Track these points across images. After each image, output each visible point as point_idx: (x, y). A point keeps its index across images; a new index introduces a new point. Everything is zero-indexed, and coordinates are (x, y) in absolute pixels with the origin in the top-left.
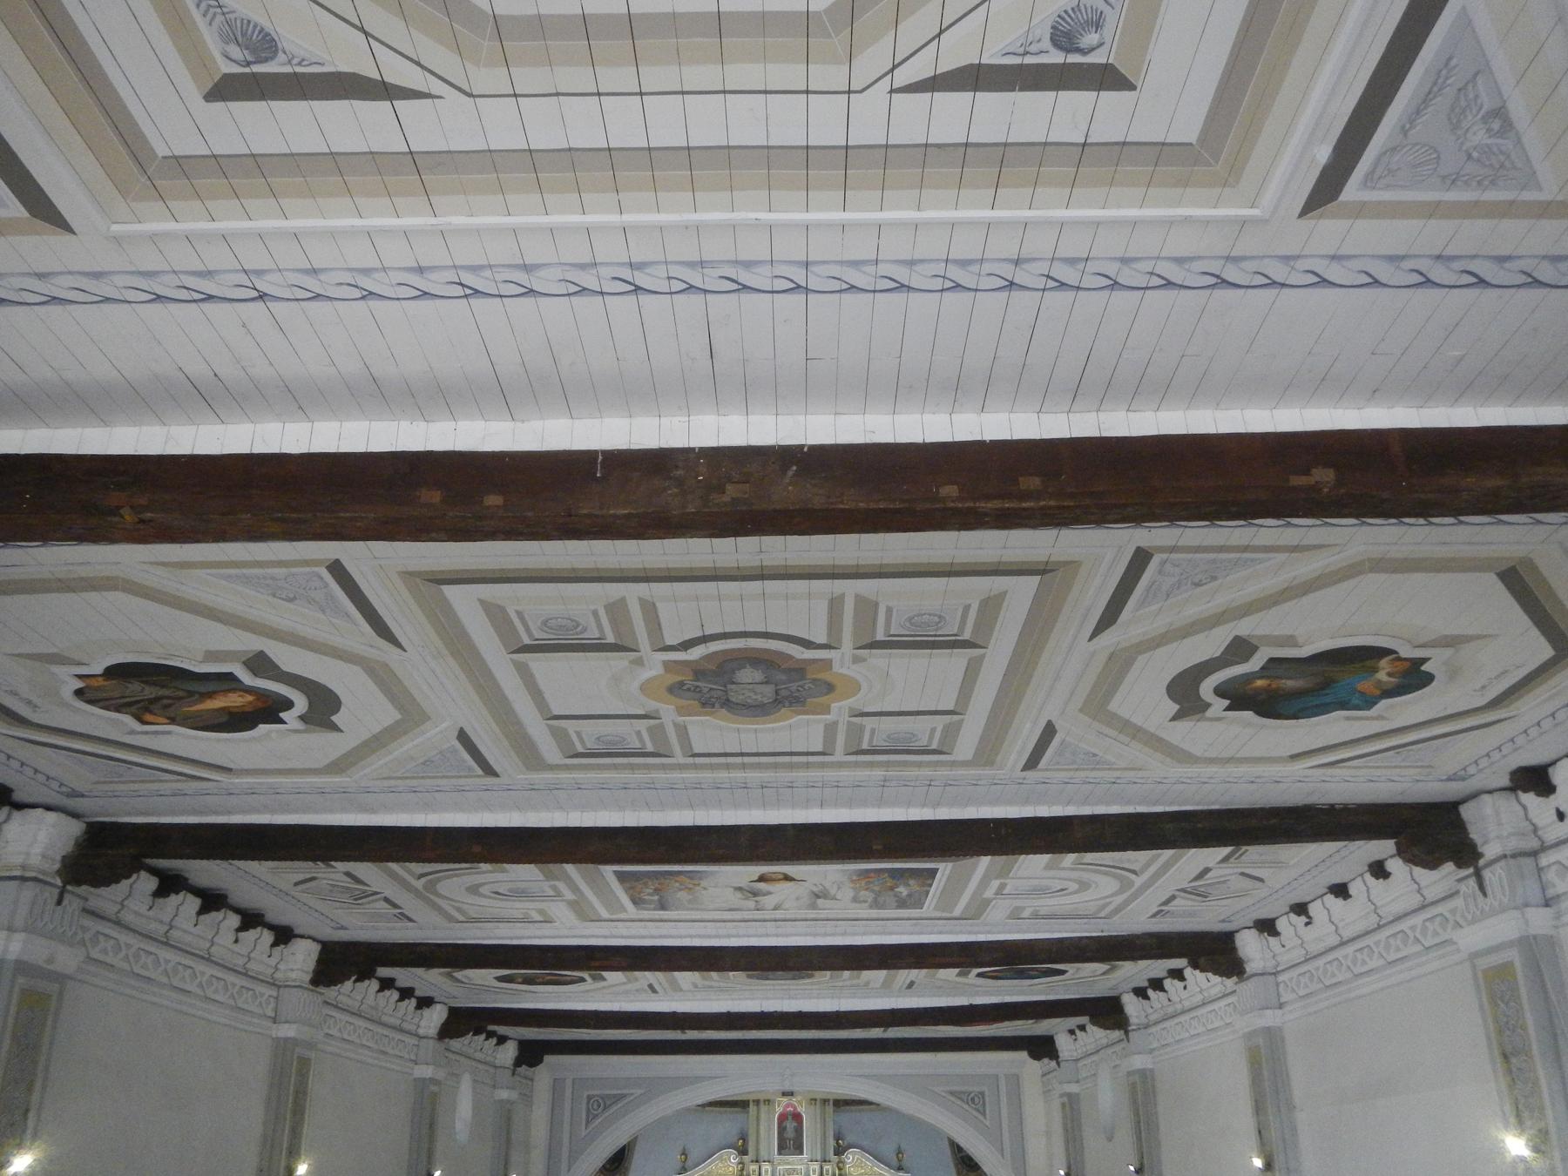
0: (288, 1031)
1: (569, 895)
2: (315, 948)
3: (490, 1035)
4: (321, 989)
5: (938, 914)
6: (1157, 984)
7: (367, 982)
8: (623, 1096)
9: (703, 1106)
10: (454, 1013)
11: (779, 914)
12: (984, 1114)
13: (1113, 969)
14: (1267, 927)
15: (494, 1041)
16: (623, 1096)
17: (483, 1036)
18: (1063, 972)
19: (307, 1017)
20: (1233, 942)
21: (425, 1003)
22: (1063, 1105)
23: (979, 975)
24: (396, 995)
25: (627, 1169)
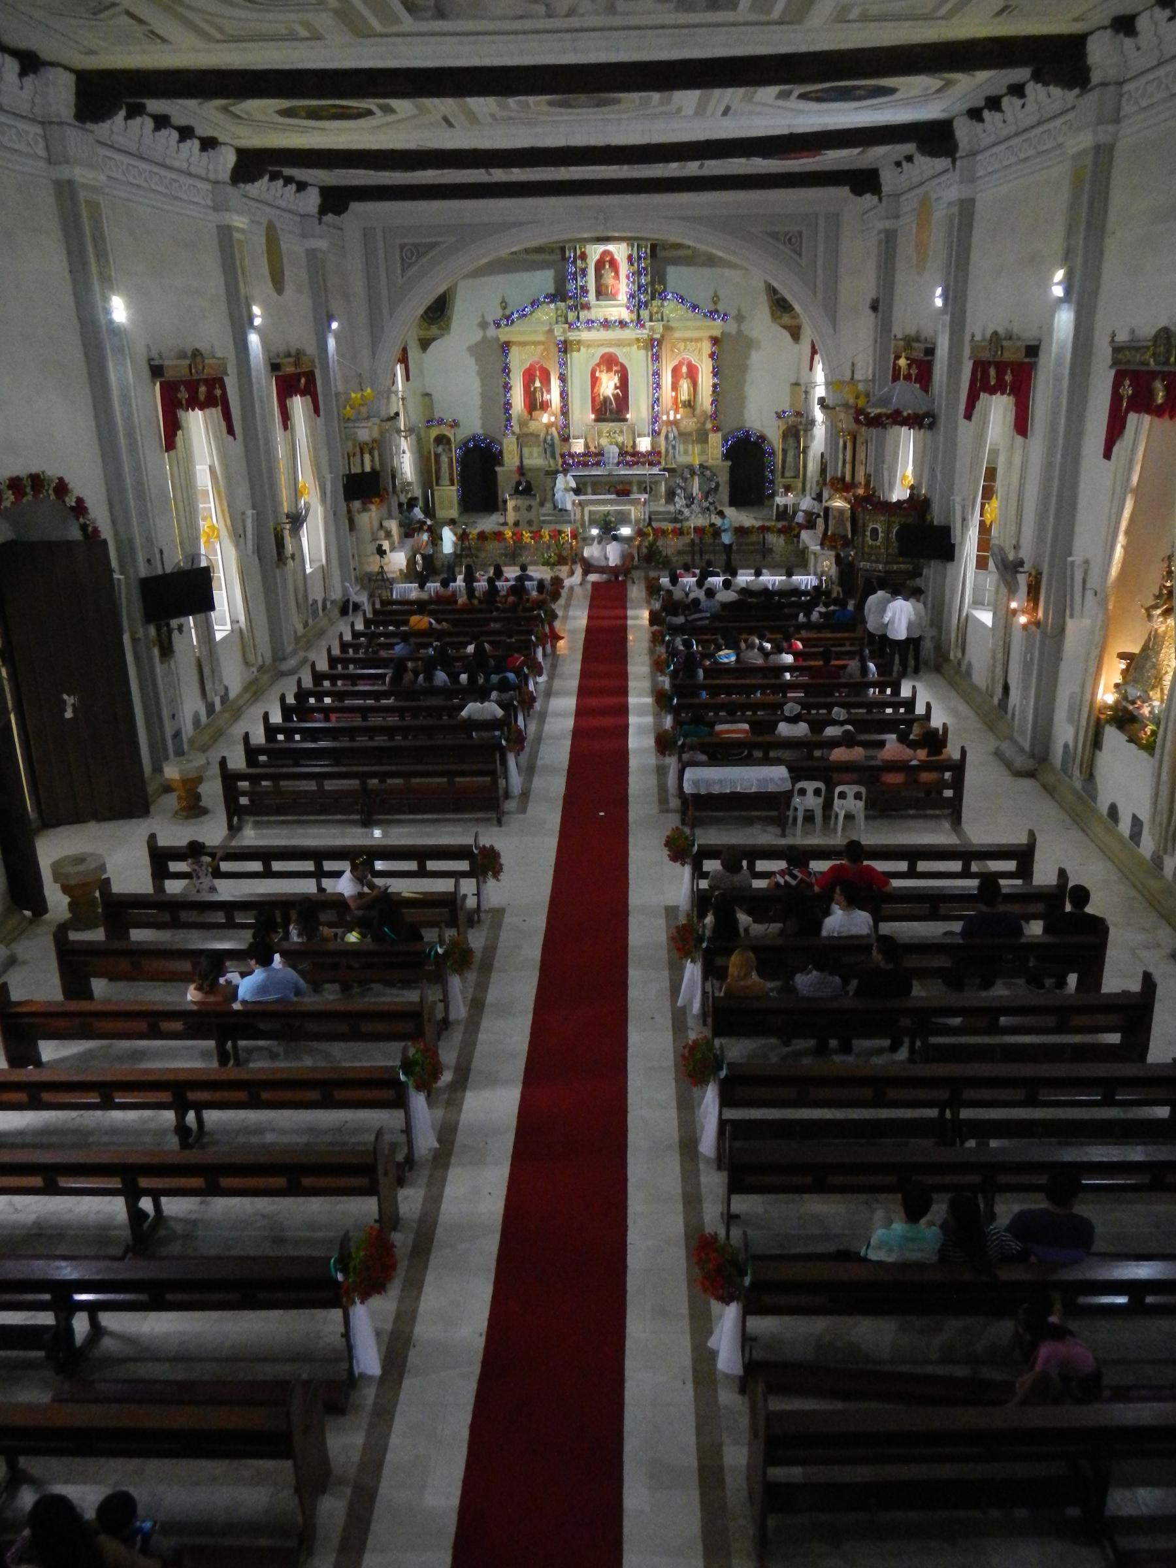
2: (69, 79)
3: (288, 180)
4: (89, 126)
5: (753, 17)
6: (994, 103)
7: (139, 120)
8: (433, 246)
10: (241, 153)
11: (574, 22)
12: (800, 255)
13: (948, 84)
14: (1125, 25)
15: (294, 187)
16: (433, 246)
17: (281, 182)
21: (209, 144)
22: (880, 242)
24: (175, 135)
25: (450, 318)
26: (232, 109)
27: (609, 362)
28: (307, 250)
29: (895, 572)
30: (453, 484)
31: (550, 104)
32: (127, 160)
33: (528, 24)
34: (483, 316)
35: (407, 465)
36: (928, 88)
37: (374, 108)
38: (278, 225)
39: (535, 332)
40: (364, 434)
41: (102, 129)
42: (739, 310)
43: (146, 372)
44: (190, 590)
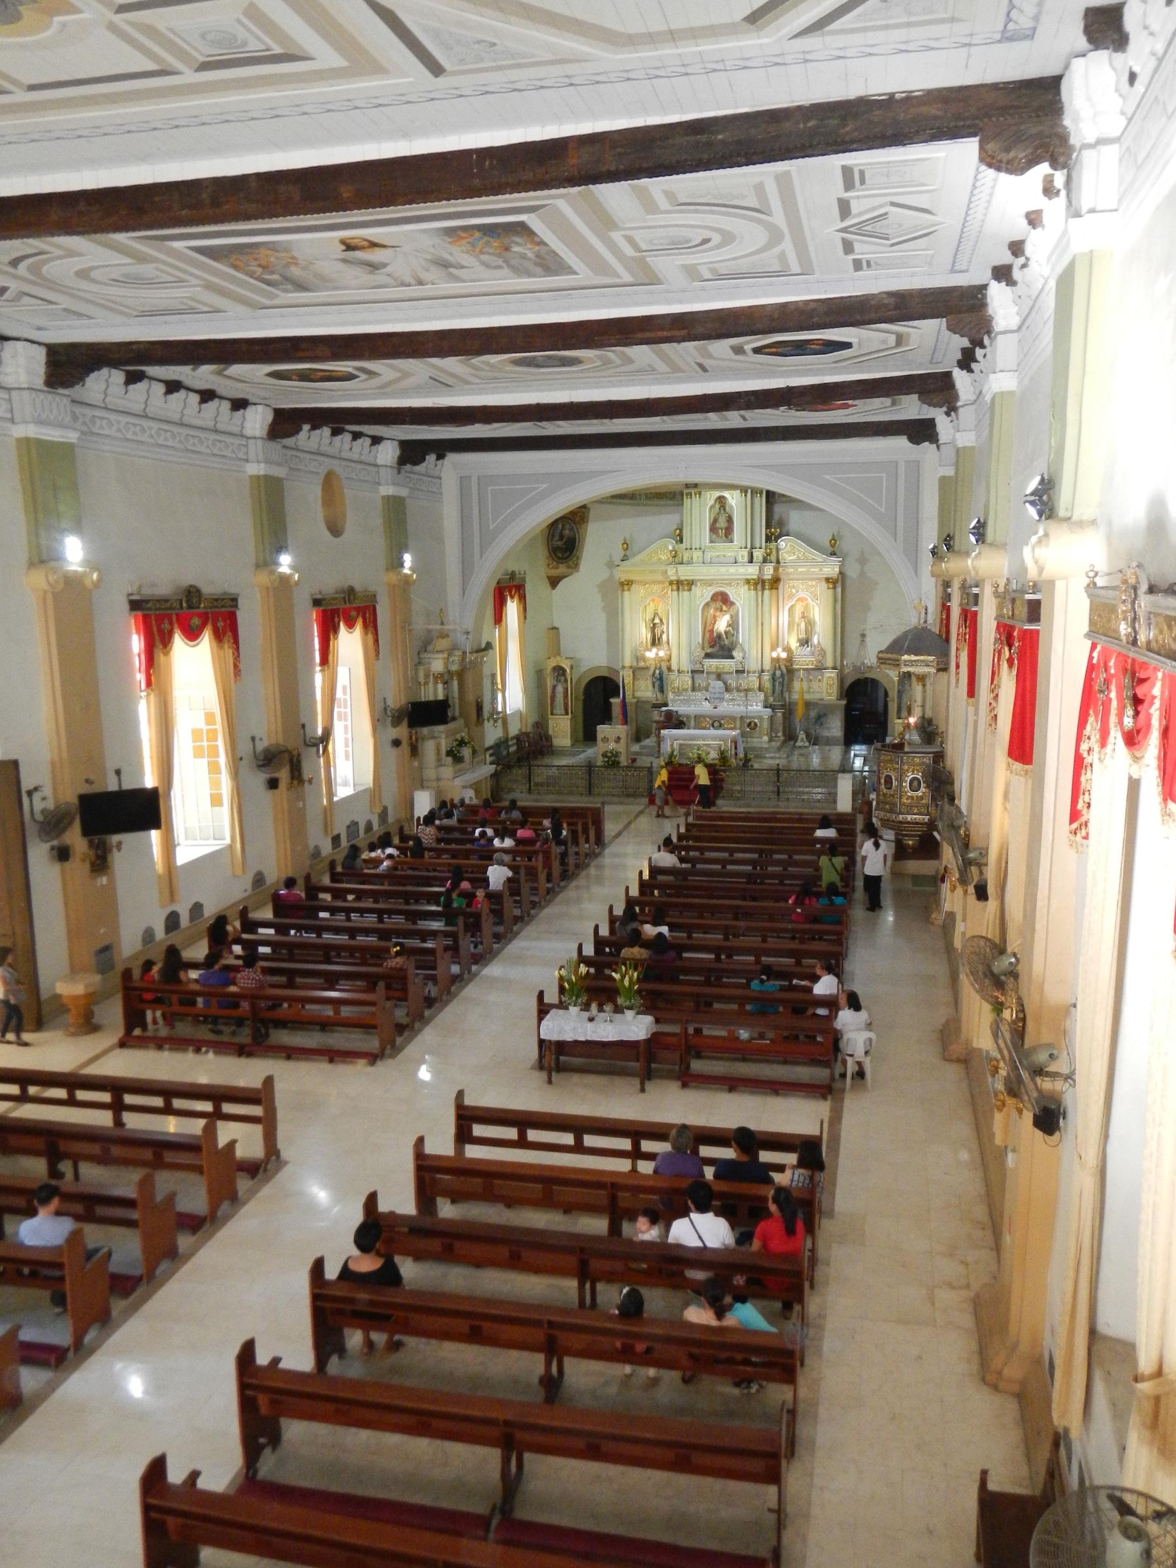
0: (31, 431)
1: (194, 281)
2: (41, 354)
3: (356, 436)
9: (613, 497)
10: (279, 414)
14: (1003, 273)
15: (368, 441)
17: (347, 437)
18: (848, 345)
19: (44, 419)
20: (985, 296)
21: (239, 404)
23: (757, 351)
24: (195, 398)
25: (578, 558)
27: (722, 599)
29: (908, 823)
30: (567, 714)
31: (517, 363)
32: (124, 419)
34: (611, 557)
35: (513, 697)
36: (884, 342)
41: (76, 391)
42: (862, 553)
43: (127, 607)
44: (145, 810)
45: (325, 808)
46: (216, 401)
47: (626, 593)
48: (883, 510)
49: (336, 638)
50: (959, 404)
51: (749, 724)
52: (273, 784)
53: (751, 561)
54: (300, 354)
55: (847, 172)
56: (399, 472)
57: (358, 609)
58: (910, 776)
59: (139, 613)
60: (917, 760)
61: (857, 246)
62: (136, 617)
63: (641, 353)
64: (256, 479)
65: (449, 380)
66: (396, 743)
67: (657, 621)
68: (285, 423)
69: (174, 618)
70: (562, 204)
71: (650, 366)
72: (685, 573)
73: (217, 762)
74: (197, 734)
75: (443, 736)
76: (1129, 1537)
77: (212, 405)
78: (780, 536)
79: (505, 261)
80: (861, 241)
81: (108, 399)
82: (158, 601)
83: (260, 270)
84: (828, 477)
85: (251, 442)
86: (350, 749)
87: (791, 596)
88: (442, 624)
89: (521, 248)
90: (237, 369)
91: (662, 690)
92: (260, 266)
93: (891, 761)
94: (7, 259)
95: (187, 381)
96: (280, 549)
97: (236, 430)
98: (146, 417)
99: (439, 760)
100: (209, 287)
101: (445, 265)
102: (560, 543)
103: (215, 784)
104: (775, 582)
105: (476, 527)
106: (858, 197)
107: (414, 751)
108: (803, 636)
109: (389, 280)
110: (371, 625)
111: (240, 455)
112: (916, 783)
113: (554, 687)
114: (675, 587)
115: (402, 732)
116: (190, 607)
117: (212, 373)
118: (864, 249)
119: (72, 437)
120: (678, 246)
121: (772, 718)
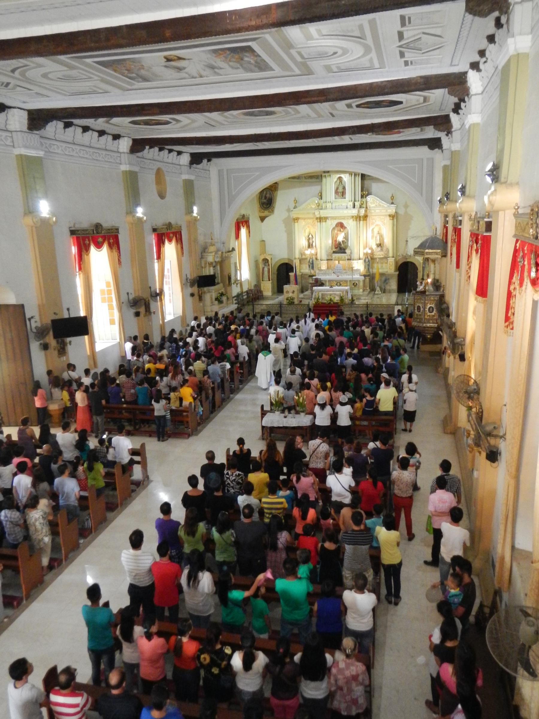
0: (24, 151)
1: (96, 78)
2: (25, 115)
3: (170, 151)
9: (289, 178)
14: (475, 66)
15: (176, 153)
19: (29, 146)
20: (466, 77)
21: (116, 137)
23: (358, 106)
24: (96, 134)
25: (274, 207)
26: (110, 122)
27: (341, 226)
28: (183, 180)
29: (428, 327)
30: (269, 280)
32: (64, 145)
33: (183, 82)
34: (289, 206)
35: (245, 273)
36: (418, 100)
37: (168, 119)
38: (164, 169)
39: (309, 213)
40: (210, 258)
41: (42, 132)
43: (69, 233)
44: (81, 326)
45: (161, 326)
46: (106, 135)
47: (296, 224)
48: (416, 182)
49: (164, 247)
50: (453, 130)
51: (354, 284)
52: (137, 314)
53: (354, 207)
54: (144, 112)
55: (402, 18)
56: (190, 168)
57: (173, 233)
58: (429, 306)
59: (75, 236)
60: (432, 298)
61: (406, 54)
62: (73, 238)
63: (304, 109)
64: (125, 172)
65: (213, 123)
66: (192, 295)
67: (310, 236)
68: (138, 145)
69: (90, 238)
70: (268, 37)
71: (308, 115)
72: (323, 213)
73: (112, 305)
74: (102, 292)
75: (213, 291)
76: (529, 626)
77: (104, 137)
78: (368, 195)
79: (241, 65)
80: (409, 52)
81: (57, 135)
82: (83, 230)
83: (127, 72)
84: (391, 167)
85: (122, 155)
86: (171, 298)
87: (373, 224)
88: (212, 239)
89: (248, 58)
90: (115, 120)
91: (313, 268)
92: (126, 70)
93: (420, 299)
94: (10, 69)
95: (92, 126)
96: (137, 204)
97: (116, 149)
98: (74, 144)
99: (212, 302)
100: (103, 80)
101: (212, 67)
102: (265, 201)
103: (112, 314)
104: (366, 217)
105: (226, 193)
106: (407, 30)
107: (200, 298)
108: (378, 242)
109: (187, 76)
110: (179, 240)
111: (118, 161)
112: (431, 309)
113: (263, 268)
114: (319, 220)
115: (195, 289)
116: (97, 233)
117: (103, 122)
118: (409, 56)
119: (41, 154)
120: (322, 56)
121: (364, 281)
